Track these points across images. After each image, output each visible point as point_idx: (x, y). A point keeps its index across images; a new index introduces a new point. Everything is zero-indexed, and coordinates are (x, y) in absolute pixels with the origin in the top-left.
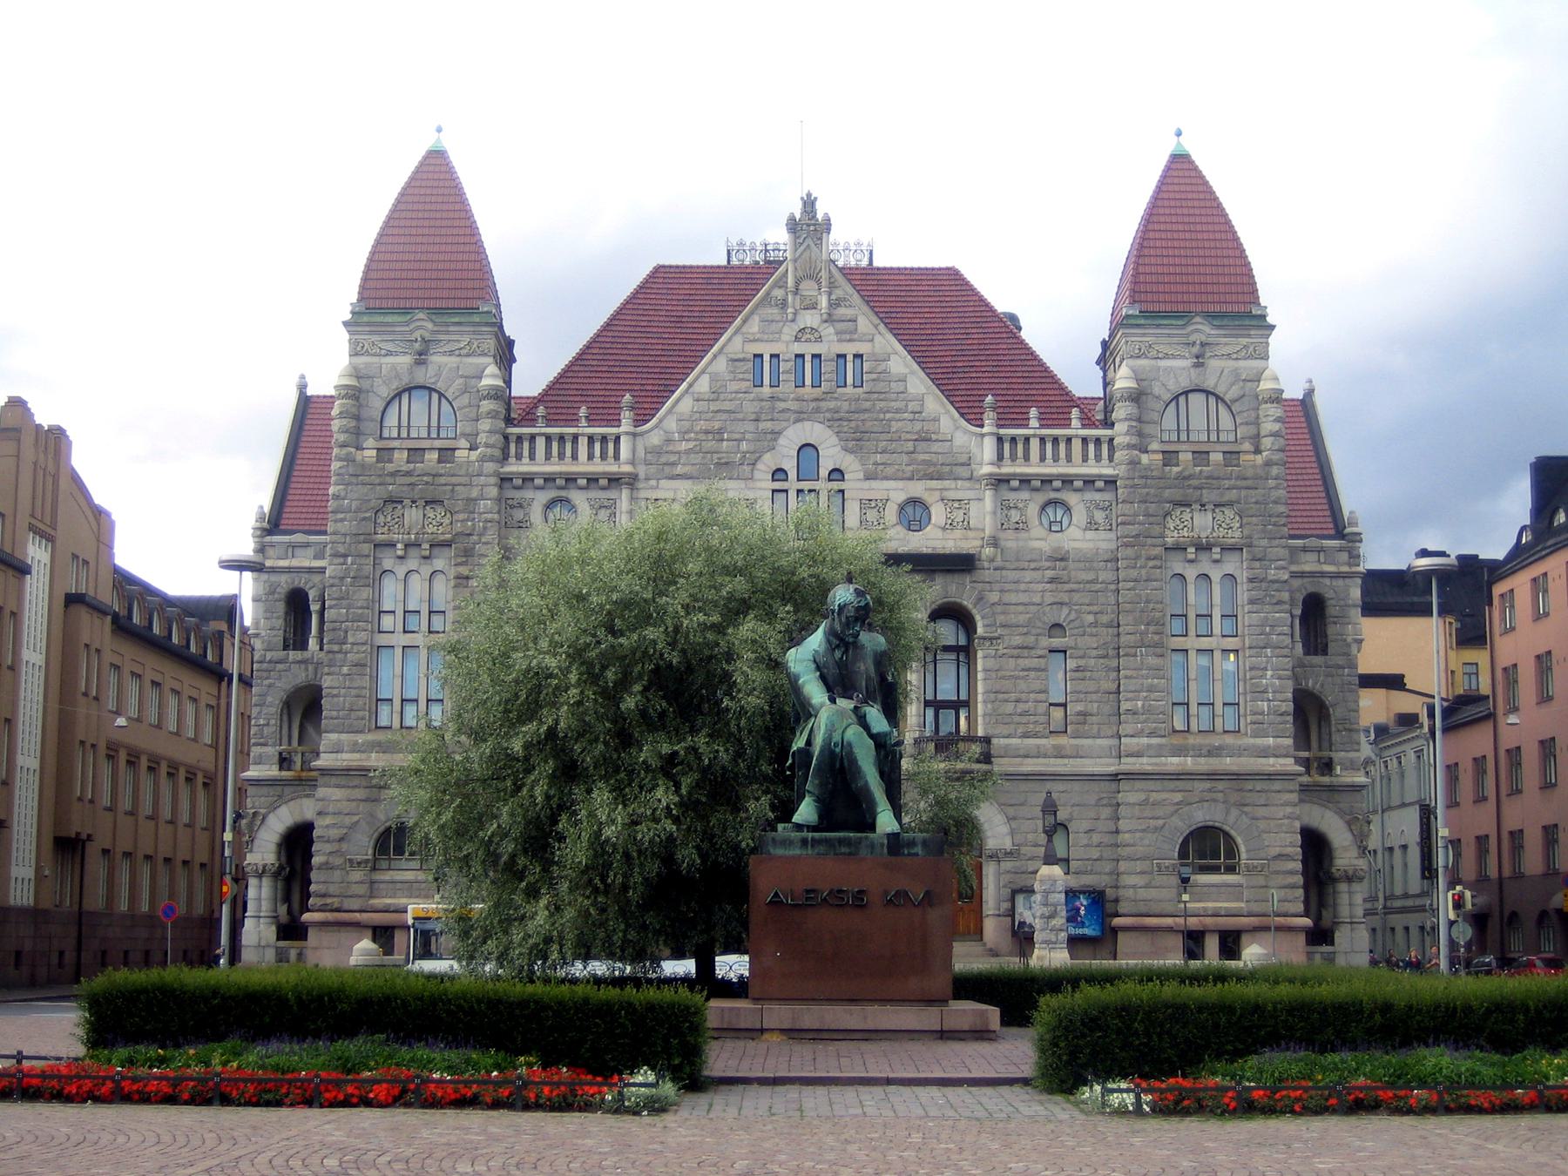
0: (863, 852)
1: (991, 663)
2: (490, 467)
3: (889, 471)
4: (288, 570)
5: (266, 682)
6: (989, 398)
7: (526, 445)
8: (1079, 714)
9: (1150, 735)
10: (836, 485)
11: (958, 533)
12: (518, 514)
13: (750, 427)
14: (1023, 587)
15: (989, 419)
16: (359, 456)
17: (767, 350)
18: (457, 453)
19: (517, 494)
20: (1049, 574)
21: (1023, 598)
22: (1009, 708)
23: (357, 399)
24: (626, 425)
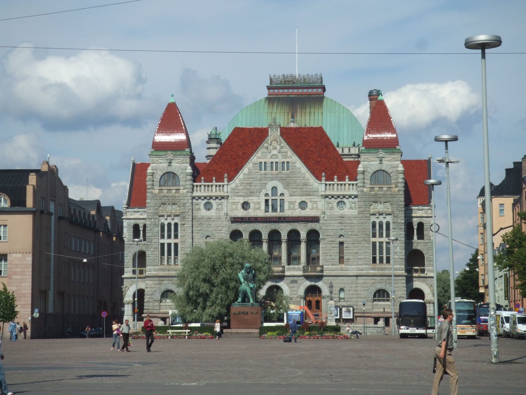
1: (323, 246)
2: (189, 194)
3: (296, 194)
6: (323, 174)
8: (347, 259)
9: (366, 265)
10: (281, 198)
11: (315, 211)
12: (197, 207)
13: (259, 182)
14: (332, 225)
15: (324, 178)
16: (154, 191)
17: (263, 161)
18: (180, 191)
20: (340, 221)
21: (332, 228)
22: (328, 258)
24: (226, 183)
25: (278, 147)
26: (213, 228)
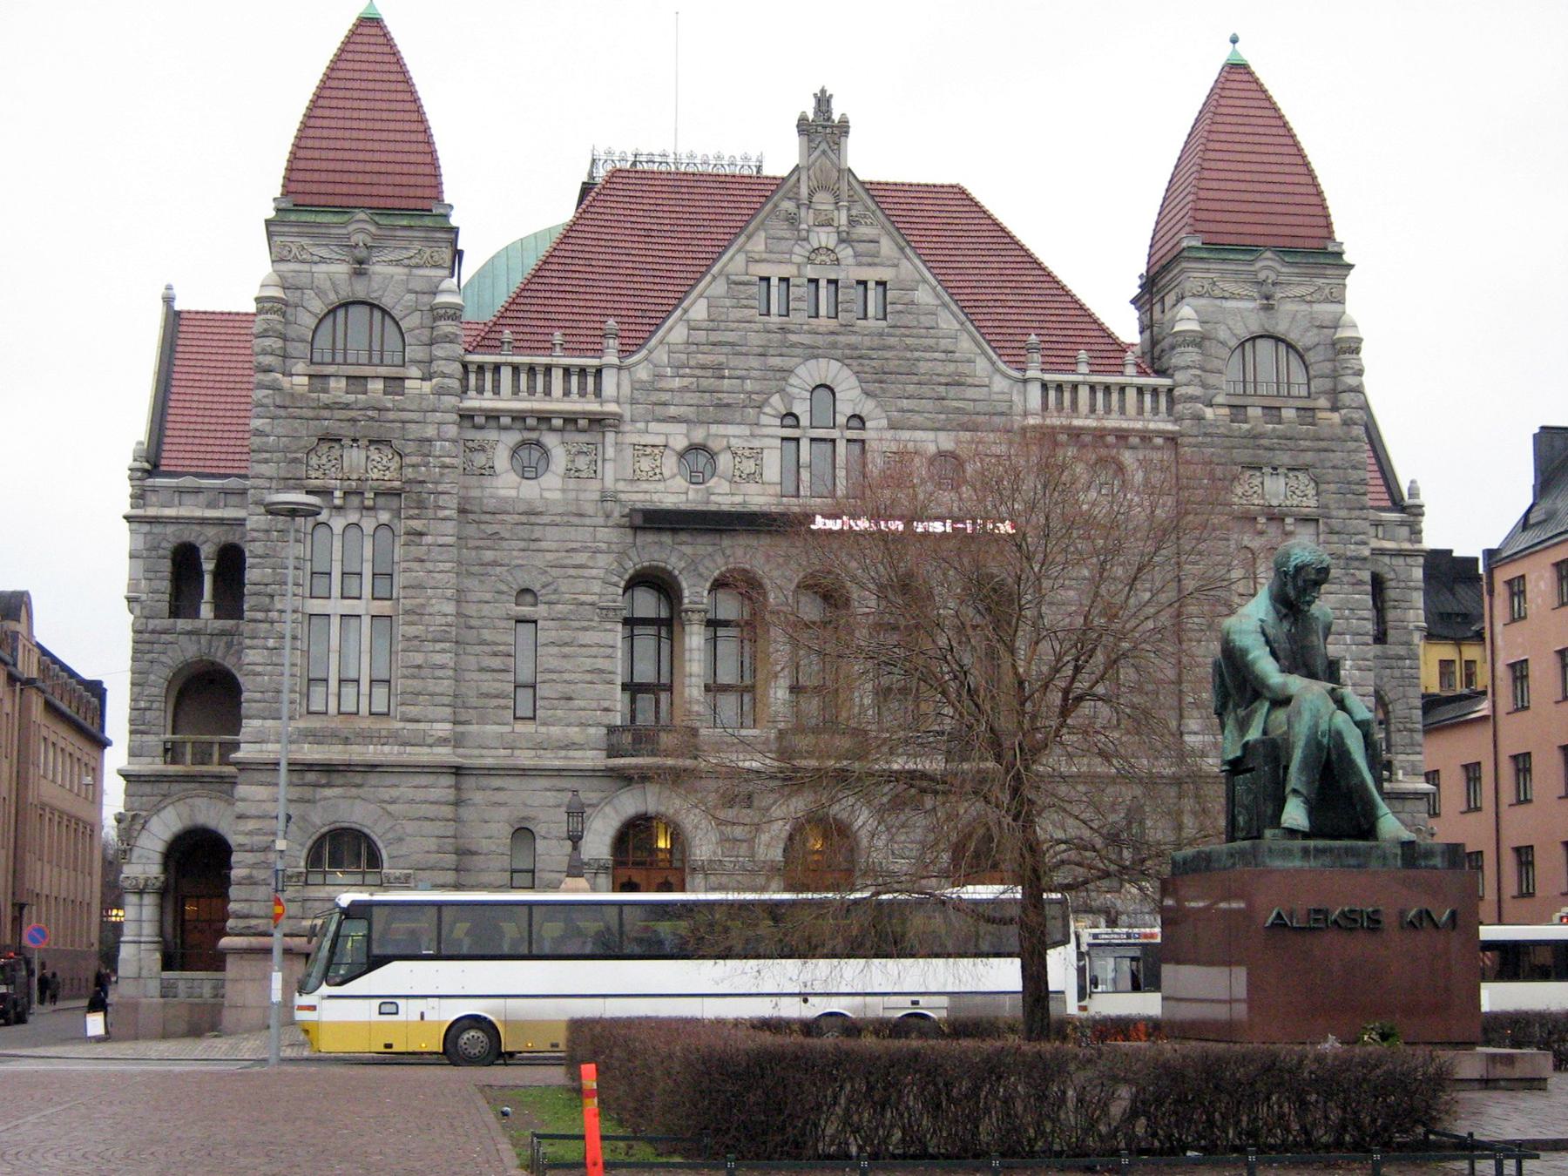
0: (1374, 864)
4: (176, 520)
5: (149, 656)
7: (489, 376)
12: (480, 460)
13: (755, 362)
16: (285, 382)
17: (775, 272)
18: (408, 383)
19: (478, 435)
23: (284, 314)
24: (611, 358)
25: (844, 220)
26: (549, 556)
